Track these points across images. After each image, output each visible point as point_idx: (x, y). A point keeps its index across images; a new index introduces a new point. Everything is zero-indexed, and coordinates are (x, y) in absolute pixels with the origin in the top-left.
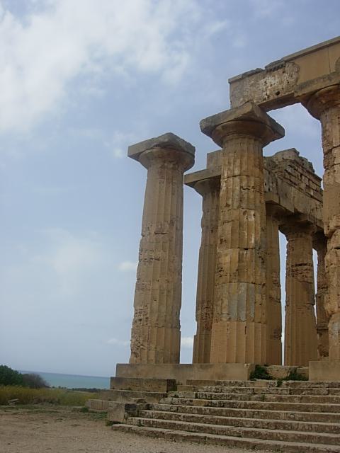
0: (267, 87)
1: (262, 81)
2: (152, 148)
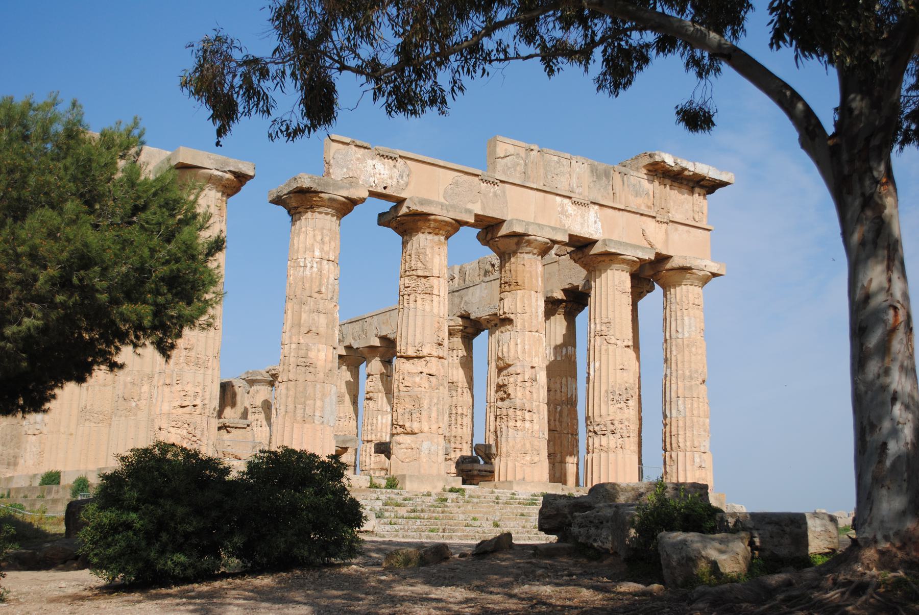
0: (375, 174)
1: (370, 162)
2: (225, 172)
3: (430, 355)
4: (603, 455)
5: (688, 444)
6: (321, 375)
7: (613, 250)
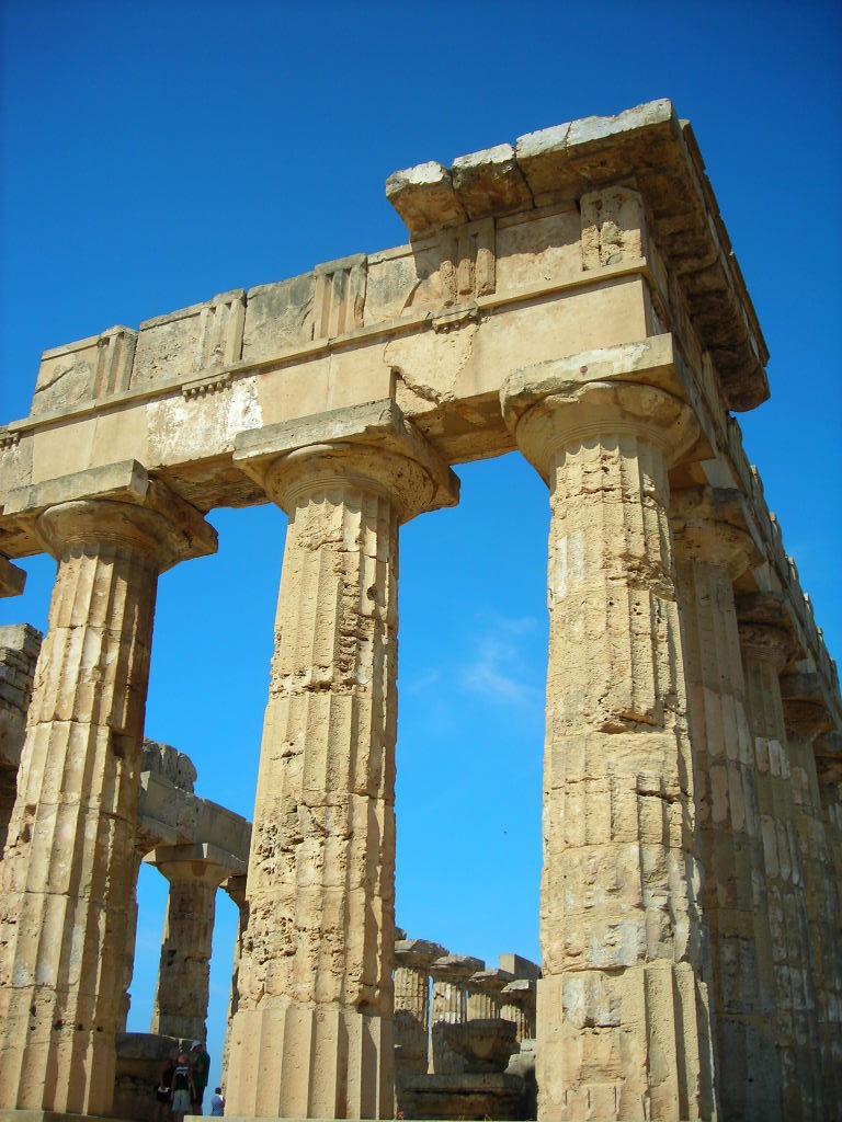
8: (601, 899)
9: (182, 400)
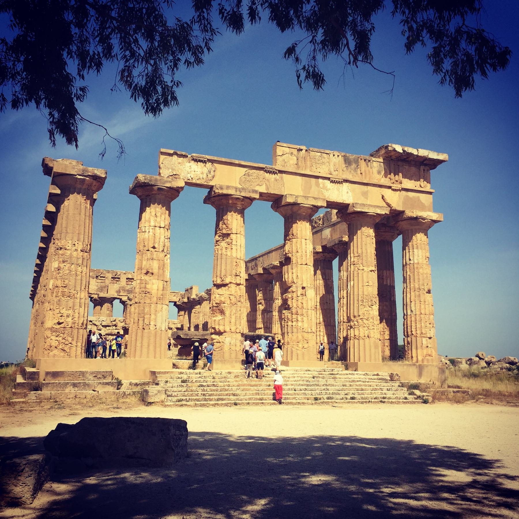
0: (192, 171)
1: (188, 164)
3: (231, 283)
4: (356, 341)
5: (418, 332)
6: (155, 299)
7: (359, 210)
8: (428, 325)
9: (329, 182)
